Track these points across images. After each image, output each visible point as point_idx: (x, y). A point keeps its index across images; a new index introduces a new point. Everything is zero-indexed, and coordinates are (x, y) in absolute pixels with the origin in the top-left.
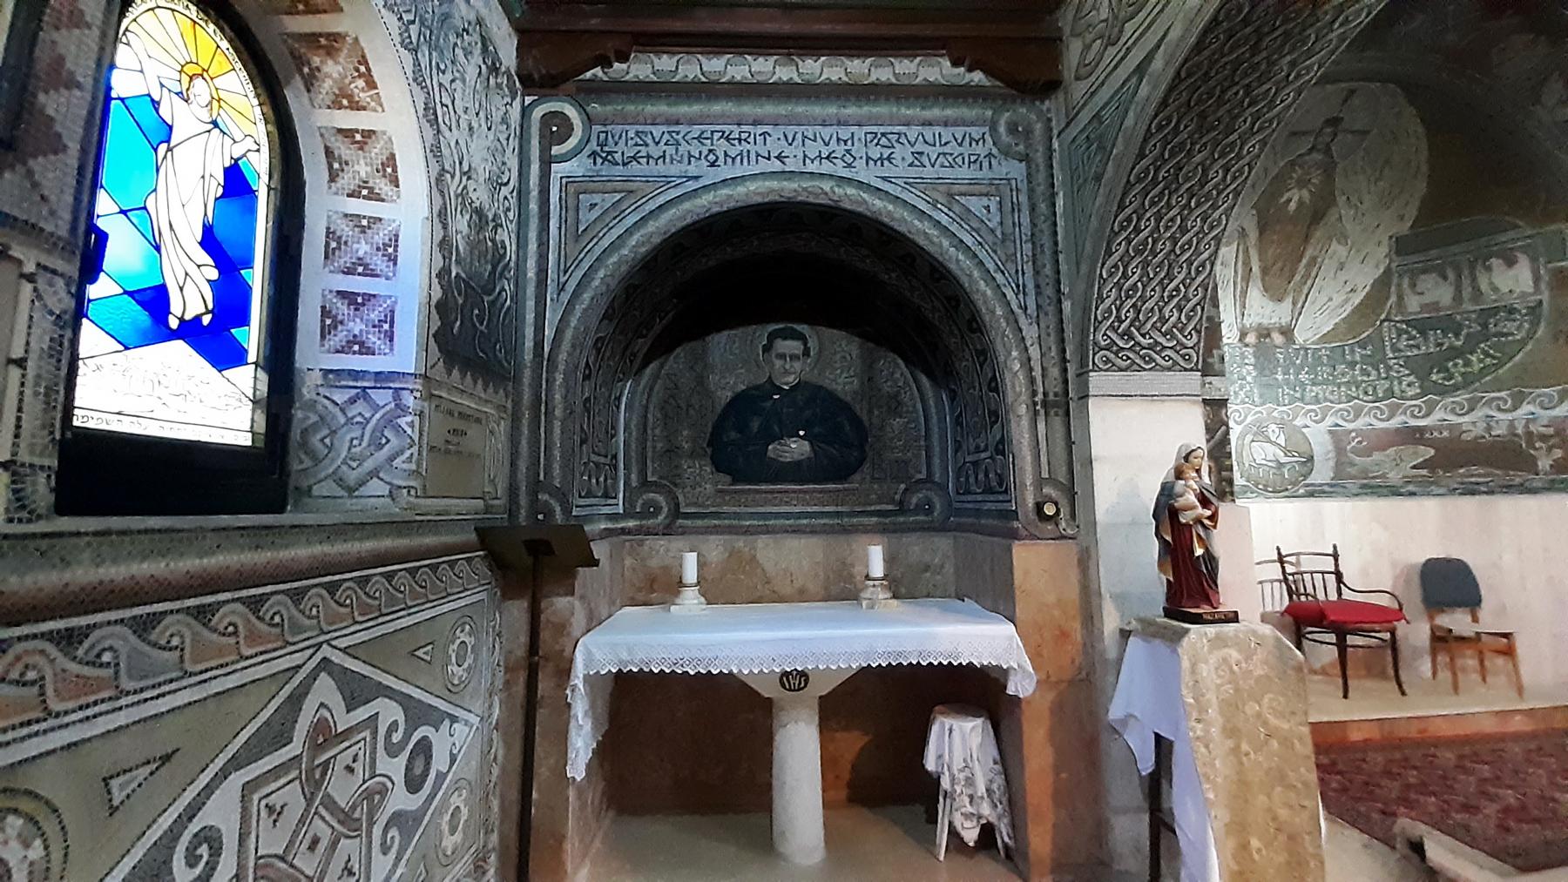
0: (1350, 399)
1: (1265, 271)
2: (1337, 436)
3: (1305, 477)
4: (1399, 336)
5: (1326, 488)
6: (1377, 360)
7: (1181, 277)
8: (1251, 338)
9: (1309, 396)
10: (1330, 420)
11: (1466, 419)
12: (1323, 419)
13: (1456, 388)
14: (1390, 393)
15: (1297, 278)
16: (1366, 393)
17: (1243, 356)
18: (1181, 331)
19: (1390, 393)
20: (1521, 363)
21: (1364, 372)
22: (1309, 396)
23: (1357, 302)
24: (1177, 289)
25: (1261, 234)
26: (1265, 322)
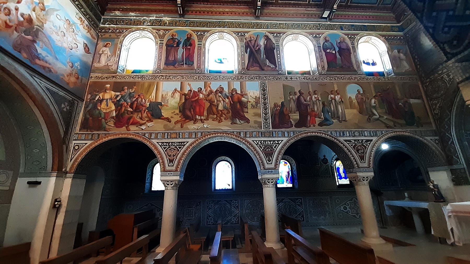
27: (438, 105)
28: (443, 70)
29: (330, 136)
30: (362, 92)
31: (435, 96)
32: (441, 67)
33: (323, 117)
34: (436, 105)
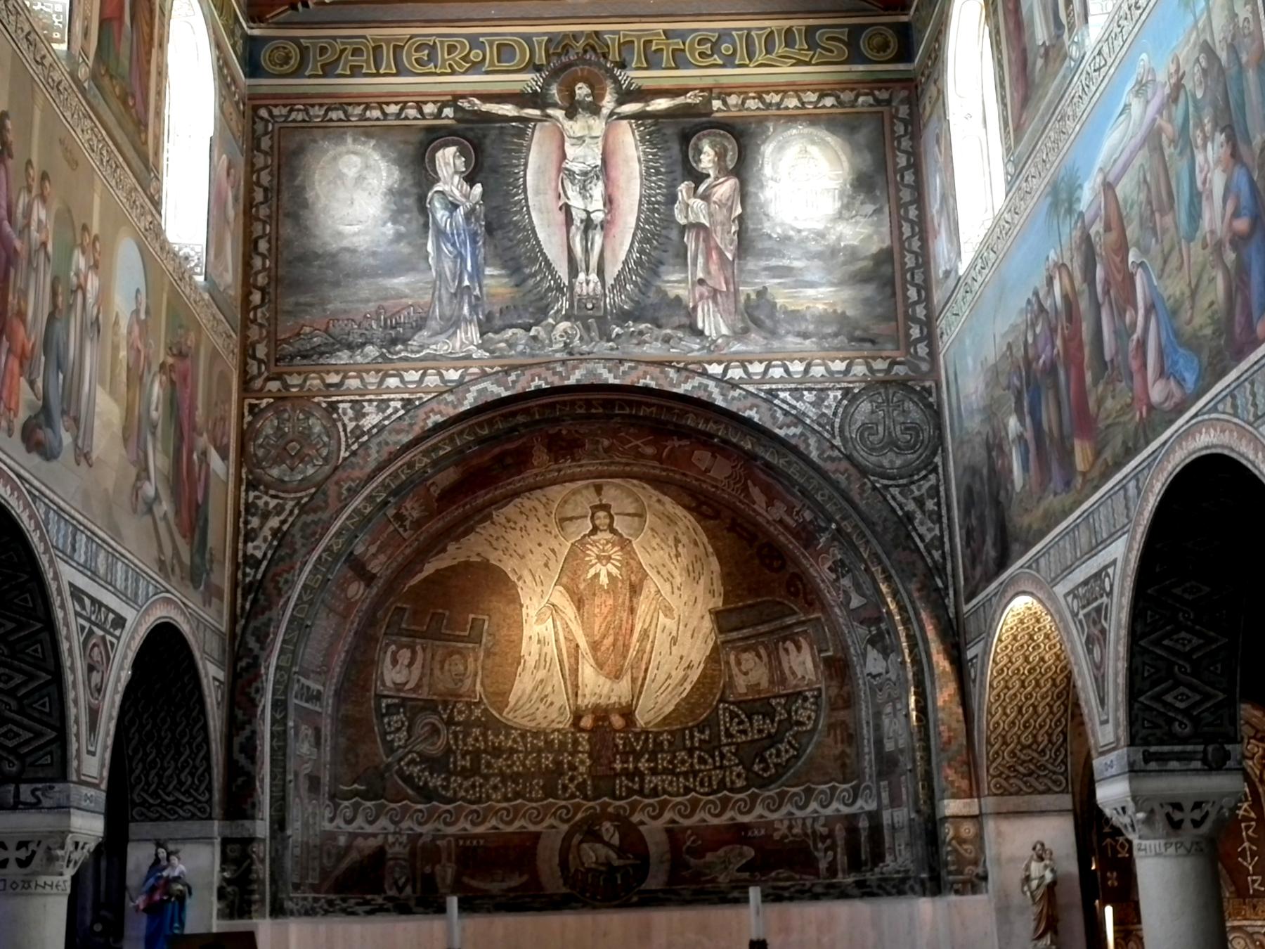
0: (687, 790)
1: (595, 646)
2: (673, 833)
3: (640, 885)
4: (732, 720)
5: (660, 895)
7: (187, 752)
8: (587, 722)
10: (667, 815)
11: (775, 816)
14: (722, 785)
15: (632, 653)
16: (702, 785)
17: (576, 742)
18: (196, 790)
19: (722, 785)
21: (702, 761)
23: (695, 679)
24: (186, 761)
25: (578, 609)
27: (274, 522)
28: (345, 377)
29: (42, 538)
30: (143, 316)
31: (275, 472)
32: (343, 357)
33: (39, 383)
34: (265, 516)
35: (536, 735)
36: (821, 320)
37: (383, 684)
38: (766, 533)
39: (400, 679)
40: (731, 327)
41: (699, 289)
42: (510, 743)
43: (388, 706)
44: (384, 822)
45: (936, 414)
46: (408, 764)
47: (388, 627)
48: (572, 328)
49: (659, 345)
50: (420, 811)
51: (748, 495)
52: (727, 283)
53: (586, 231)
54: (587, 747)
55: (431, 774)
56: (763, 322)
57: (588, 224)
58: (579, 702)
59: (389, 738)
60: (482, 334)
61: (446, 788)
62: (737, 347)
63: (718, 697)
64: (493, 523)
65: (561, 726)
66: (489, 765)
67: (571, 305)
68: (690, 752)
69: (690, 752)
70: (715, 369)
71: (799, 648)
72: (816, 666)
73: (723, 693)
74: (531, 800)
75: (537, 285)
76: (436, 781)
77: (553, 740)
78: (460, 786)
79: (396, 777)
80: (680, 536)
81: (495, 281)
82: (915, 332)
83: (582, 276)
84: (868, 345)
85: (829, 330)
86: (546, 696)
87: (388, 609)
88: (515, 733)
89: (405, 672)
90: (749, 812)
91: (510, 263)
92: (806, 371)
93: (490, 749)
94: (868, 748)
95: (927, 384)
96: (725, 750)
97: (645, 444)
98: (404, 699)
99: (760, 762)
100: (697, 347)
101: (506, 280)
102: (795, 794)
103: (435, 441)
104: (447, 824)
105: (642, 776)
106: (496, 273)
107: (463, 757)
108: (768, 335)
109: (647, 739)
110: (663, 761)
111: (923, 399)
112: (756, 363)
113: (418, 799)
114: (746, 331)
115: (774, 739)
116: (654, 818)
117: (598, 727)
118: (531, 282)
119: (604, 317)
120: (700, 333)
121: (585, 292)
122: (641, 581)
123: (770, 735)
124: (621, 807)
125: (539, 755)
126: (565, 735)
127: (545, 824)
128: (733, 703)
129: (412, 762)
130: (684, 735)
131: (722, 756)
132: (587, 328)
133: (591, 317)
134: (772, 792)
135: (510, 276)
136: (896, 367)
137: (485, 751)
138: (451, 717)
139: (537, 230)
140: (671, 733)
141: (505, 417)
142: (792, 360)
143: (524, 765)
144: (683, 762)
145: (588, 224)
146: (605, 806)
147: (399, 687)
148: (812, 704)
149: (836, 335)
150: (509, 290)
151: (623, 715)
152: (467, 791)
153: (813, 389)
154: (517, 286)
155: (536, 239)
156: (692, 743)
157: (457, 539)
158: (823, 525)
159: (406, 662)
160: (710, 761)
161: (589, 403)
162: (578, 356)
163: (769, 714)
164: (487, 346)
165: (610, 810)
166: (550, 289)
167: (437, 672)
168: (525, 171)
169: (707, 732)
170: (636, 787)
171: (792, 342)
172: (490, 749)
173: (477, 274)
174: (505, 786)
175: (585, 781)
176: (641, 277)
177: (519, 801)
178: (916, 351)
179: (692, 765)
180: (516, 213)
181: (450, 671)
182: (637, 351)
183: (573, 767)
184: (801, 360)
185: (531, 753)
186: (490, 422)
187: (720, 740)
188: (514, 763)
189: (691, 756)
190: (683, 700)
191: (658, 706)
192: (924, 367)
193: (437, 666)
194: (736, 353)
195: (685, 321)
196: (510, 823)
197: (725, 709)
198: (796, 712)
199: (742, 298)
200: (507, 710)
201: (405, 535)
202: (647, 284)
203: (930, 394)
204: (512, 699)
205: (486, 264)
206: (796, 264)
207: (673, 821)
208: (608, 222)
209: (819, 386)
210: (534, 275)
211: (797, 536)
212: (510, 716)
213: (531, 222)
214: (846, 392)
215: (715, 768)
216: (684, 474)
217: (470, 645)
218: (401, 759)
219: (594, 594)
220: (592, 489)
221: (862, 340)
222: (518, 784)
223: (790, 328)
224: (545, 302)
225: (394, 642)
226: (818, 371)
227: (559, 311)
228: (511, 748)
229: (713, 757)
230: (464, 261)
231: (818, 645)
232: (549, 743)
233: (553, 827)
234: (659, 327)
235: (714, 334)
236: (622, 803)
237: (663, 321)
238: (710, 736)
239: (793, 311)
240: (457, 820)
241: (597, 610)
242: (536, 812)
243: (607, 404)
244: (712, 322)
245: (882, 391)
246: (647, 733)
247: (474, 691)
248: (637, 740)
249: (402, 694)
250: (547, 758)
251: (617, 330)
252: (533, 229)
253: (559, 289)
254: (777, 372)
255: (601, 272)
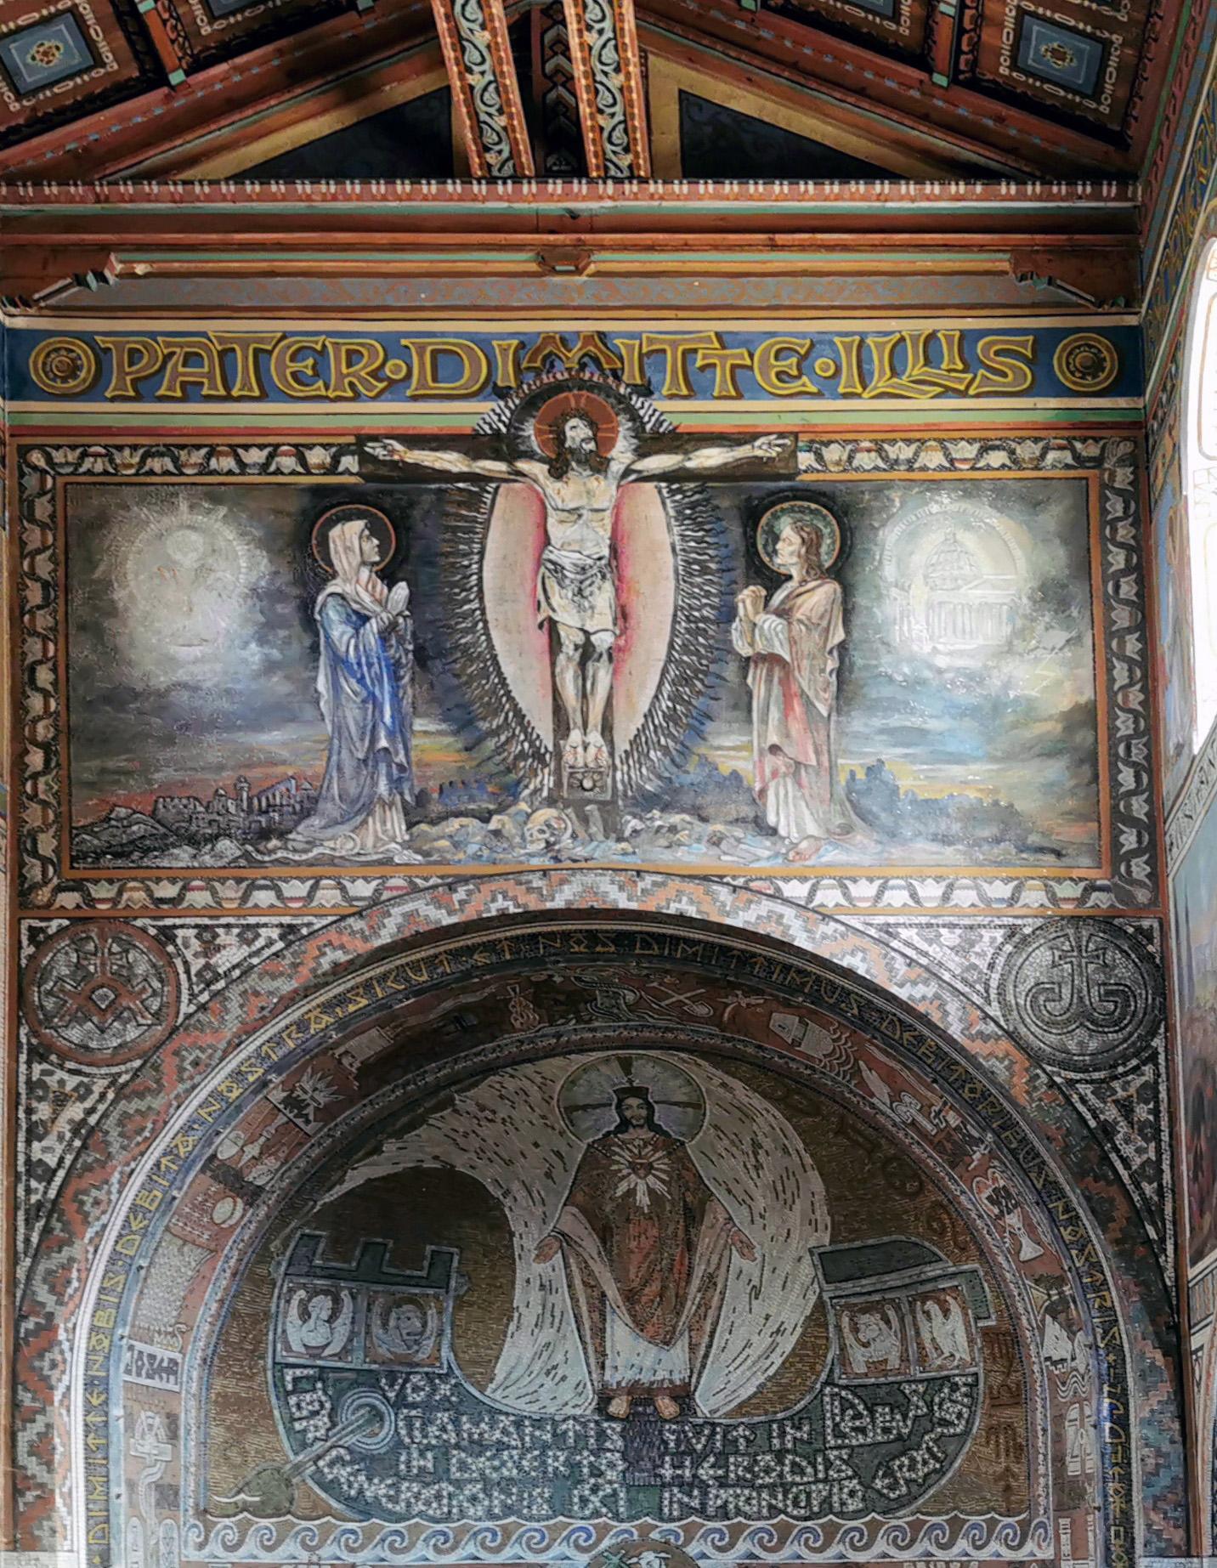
0: (774, 1511)
4: (843, 1411)
6: (812, 1450)
8: (619, 1407)
9: (712, 1505)
10: (742, 1547)
12: (732, 1545)
13: (901, 1503)
14: (827, 1506)
16: (796, 1504)
17: (601, 1435)
19: (827, 1506)
20: (960, 1473)
21: (797, 1469)
22: (712, 1505)
26: (645, 1378)
35: (538, 1423)
36: (972, 816)
37: (288, 1348)
38: (893, 1141)
39: (315, 1340)
40: (822, 823)
41: (771, 761)
42: (497, 1435)
43: (296, 1380)
44: (290, 1547)
45: (1158, 972)
46: (331, 1464)
47: (289, 1265)
48: (559, 818)
49: (702, 848)
50: (353, 1532)
51: (862, 1083)
52: (817, 753)
53: (582, 665)
54: (620, 1443)
55: (370, 1479)
56: (877, 818)
57: (587, 651)
58: (607, 1377)
59: (298, 1426)
60: (410, 826)
61: (394, 1499)
62: (831, 855)
63: (823, 1376)
64: (456, 1111)
65: (578, 1412)
66: (463, 1466)
67: (559, 783)
68: (780, 1456)
69: (780, 1456)
70: (796, 890)
71: (946, 1313)
72: (971, 1341)
73: (831, 1371)
74: (531, 1518)
75: (500, 749)
76: (377, 1489)
77: (565, 1432)
78: (417, 1496)
79: (310, 1483)
80: (760, 1138)
81: (433, 744)
82: (1129, 840)
83: (575, 736)
84: (1050, 859)
85: (987, 832)
86: (555, 1367)
87: (289, 1238)
88: (504, 1421)
89: (324, 1329)
90: (867, 1547)
91: (456, 713)
92: (946, 897)
93: (465, 1443)
94: (1044, 1468)
95: (1146, 924)
96: (832, 1455)
97: (693, 999)
98: (322, 1368)
99: (884, 1476)
100: (767, 853)
101: (451, 739)
102: (934, 1526)
103: (341, 989)
104: (392, 1548)
105: (704, 1488)
106: (432, 727)
107: (422, 1454)
108: (885, 838)
109: (713, 1433)
110: (737, 1467)
111: (1138, 947)
112: (863, 882)
113: (349, 1514)
114: (847, 829)
115: (905, 1445)
116: (721, 1549)
117: (636, 1414)
118: (491, 744)
119: (613, 802)
120: (774, 832)
121: (580, 763)
122: (703, 1203)
123: (900, 1437)
124: (670, 1531)
125: (543, 1453)
126: (584, 1425)
127: (551, 1553)
128: (846, 1387)
129: (339, 1459)
130: (770, 1431)
131: (828, 1465)
132: (585, 820)
133: (590, 802)
134: (903, 1519)
135: (456, 733)
136: (1095, 895)
137: (457, 1446)
138: (401, 1395)
139: (500, 658)
140: (752, 1427)
141: (455, 955)
142: (923, 880)
143: (520, 1468)
144: (767, 1471)
145: (587, 651)
146: (645, 1530)
147: (314, 1352)
148: (966, 1395)
149: (997, 841)
150: (456, 757)
151: (674, 1398)
152: (428, 1503)
153: (955, 926)
154: (467, 749)
155: (500, 674)
156: (782, 1443)
157: (399, 1134)
158: (976, 1135)
159: (325, 1315)
160: (809, 1470)
161: (592, 936)
162: (569, 864)
163: (900, 1405)
164: (417, 844)
165: (655, 1535)
166: (522, 755)
167: (377, 1330)
168: (481, 562)
169: (806, 1428)
170: (695, 1503)
171: (923, 850)
172: (465, 1443)
173: (401, 729)
174: (490, 1496)
175: (615, 1493)
176: (674, 738)
177: (513, 1519)
178: (1129, 872)
179: (781, 1475)
180: (466, 631)
181: (398, 1327)
182: (666, 858)
183: (596, 1472)
184: (938, 879)
185: (529, 1450)
186: (431, 962)
187: (825, 1441)
188: (503, 1464)
189: (781, 1462)
190: (770, 1379)
191: (730, 1387)
192: (1142, 896)
193: (376, 1322)
194: (828, 865)
195: (747, 811)
196: (497, 1550)
197: (832, 1395)
198: (941, 1405)
199: (842, 778)
200: (492, 1386)
201: (308, 1129)
202: (685, 751)
203: (1150, 940)
204: (500, 1371)
205: (415, 713)
206: (933, 725)
207: (752, 1556)
208: (620, 649)
209: (967, 921)
210: (495, 733)
211: (938, 1147)
212: (498, 1395)
213: (491, 647)
214: (1012, 931)
215: (817, 1481)
216: (760, 1047)
217: (431, 1291)
218: (319, 1457)
219: (628, 1220)
220: (615, 1064)
221: (1041, 850)
222: (510, 1495)
223: (922, 828)
224: (513, 776)
225: (304, 1286)
226: (965, 897)
227: (537, 791)
228: (499, 1442)
229: (815, 1467)
230: (378, 706)
231: (975, 1309)
232: (559, 1437)
233: (567, 1558)
234: (704, 820)
235: (795, 835)
236: (672, 1526)
237: (711, 811)
238: (810, 1434)
239: (926, 801)
240: (412, 1545)
241: (634, 1244)
242: (538, 1536)
243: (621, 938)
244: (791, 812)
245: (1071, 932)
246: (714, 1425)
247: (438, 1359)
248: (698, 1434)
249: (319, 1363)
250: (556, 1458)
251: (634, 823)
252: (494, 658)
253: (539, 756)
254: (897, 897)
255: (607, 729)
